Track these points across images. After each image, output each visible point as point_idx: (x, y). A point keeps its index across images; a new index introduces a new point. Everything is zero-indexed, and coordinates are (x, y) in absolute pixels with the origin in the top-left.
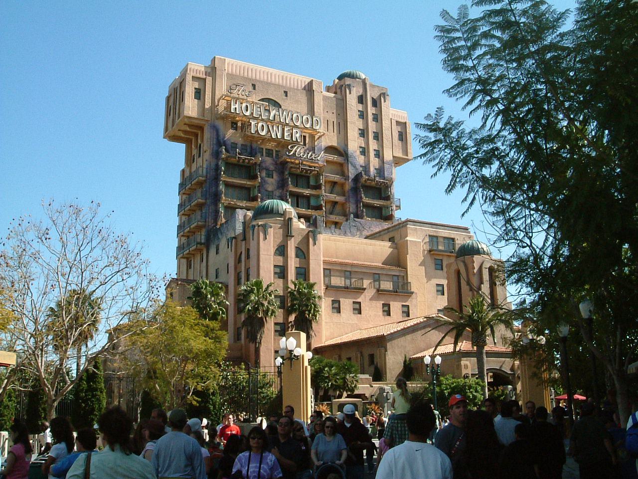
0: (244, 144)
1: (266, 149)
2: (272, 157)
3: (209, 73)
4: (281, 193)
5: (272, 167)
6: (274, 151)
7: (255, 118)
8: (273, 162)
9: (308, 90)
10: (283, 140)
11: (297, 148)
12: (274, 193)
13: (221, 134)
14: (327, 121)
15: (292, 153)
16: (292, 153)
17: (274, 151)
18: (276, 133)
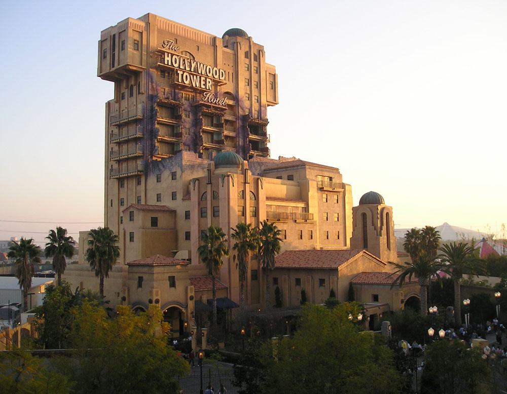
7: (181, 70)
18: (196, 83)
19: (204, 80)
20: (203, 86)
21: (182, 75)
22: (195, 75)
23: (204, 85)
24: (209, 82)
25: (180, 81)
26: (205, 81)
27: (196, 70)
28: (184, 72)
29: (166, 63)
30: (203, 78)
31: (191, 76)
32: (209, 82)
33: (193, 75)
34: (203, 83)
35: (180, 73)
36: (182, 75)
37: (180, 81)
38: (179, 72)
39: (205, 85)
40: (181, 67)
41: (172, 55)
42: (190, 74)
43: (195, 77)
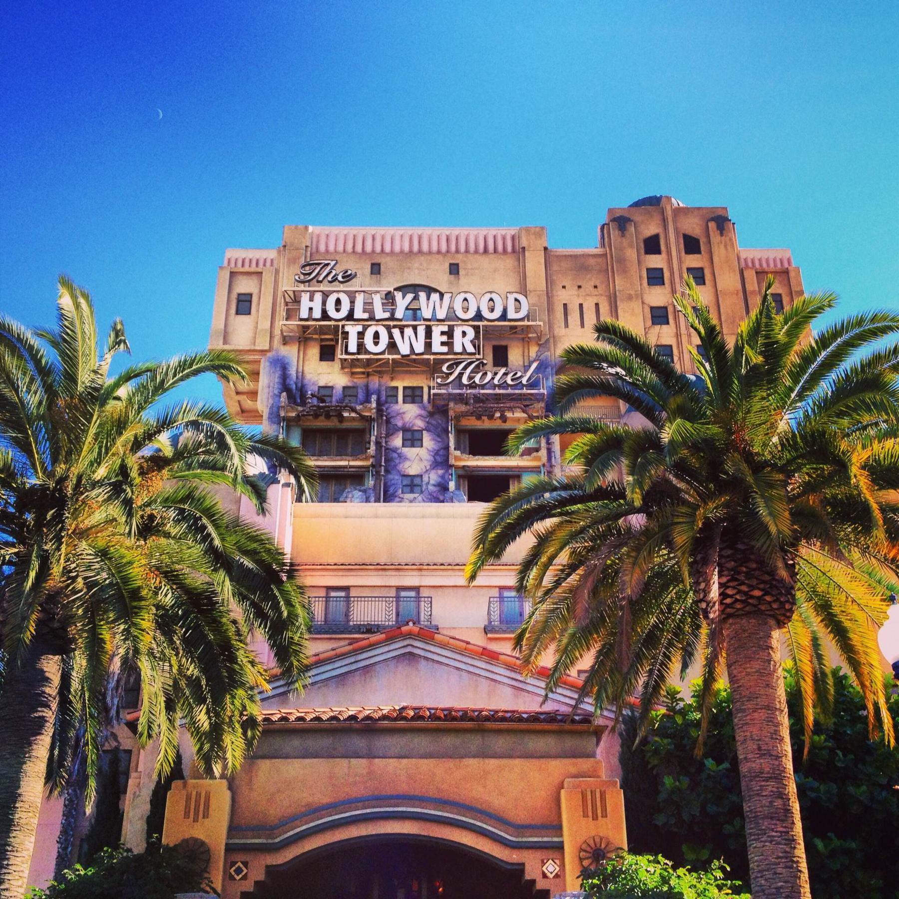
0: (350, 384)
1: (405, 388)
2: (422, 402)
3: (272, 260)
4: (442, 477)
5: (420, 424)
6: (426, 390)
8: (423, 413)
9: (514, 251)
10: (432, 357)
11: (465, 368)
12: (425, 479)
13: (293, 372)
14: (565, 305)
15: (451, 378)
16: (451, 378)
17: (426, 390)
19: (443, 333)
20: (437, 347)
21: (361, 335)
22: (408, 326)
23: (443, 344)
24: (464, 334)
25: (353, 347)
26: (450, 334)
27: (414, 312)
28: (365, 328)
29: (304, 314)
30: (437, 331)
31: (396, 332)
32: (464, 334)
33: (402, 329)
34: (437, 339)
35: (353, 330)
36: (361, 335)
37: (353, 347)
38: (347, 329)
39: (449, 344)
40: (359, 314)
41: (326, 295)
42: (388, 328)
43: (409, 332)
